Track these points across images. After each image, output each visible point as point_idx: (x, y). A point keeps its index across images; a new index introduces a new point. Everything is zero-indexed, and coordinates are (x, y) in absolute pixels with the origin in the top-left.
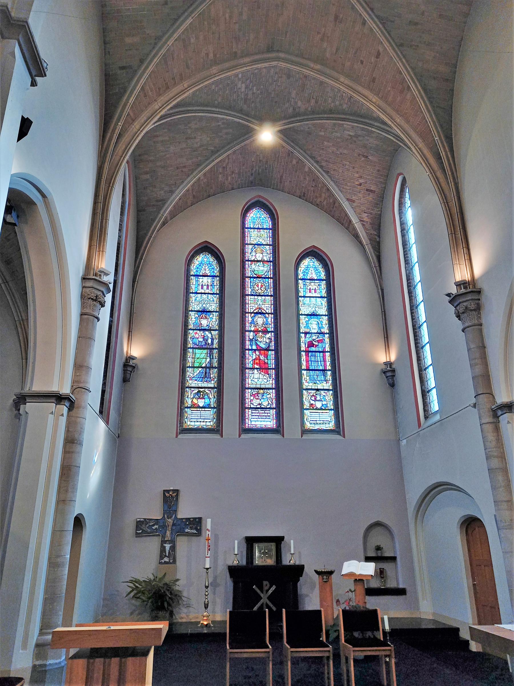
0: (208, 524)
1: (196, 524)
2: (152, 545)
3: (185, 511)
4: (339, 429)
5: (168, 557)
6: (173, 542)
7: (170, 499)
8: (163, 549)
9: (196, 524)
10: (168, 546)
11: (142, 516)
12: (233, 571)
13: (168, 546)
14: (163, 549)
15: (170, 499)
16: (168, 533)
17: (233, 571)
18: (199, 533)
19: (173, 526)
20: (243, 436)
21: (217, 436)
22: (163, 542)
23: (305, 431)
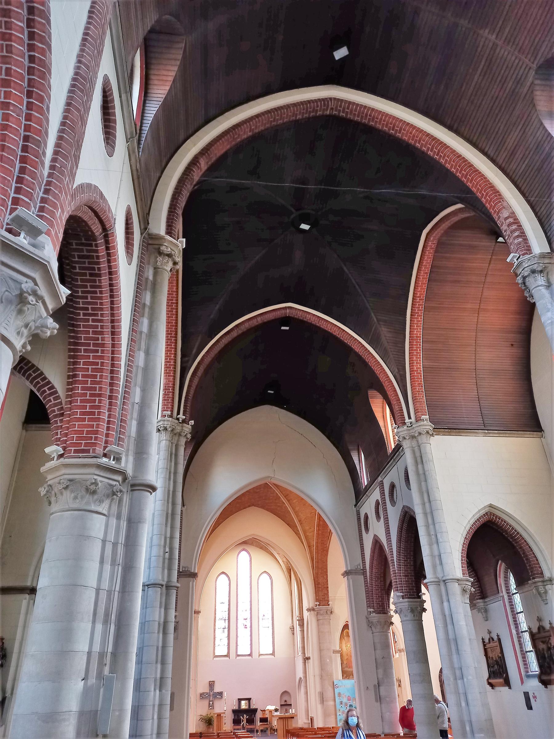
0: (225, 694)
1: (221, 694)
2: (206, 702)
3: (217, 689)
4: (273, 654)
5: (211, 706)
6: (212, 701)
7: (211, 684)
8: (210, 704)
9: (221, 694)
10: (211, 703)
11: (201, 691)
12: (234, 711)
13: (211, 703)
14: (210, 704)
15: (211, 684)
16: (211, 698)
17: (234, 711)
18: (222, 697)
19: (212, 695)
20: (237, 658)
21: (227, 658)
22: (210, 701)
23: (260, 655)
